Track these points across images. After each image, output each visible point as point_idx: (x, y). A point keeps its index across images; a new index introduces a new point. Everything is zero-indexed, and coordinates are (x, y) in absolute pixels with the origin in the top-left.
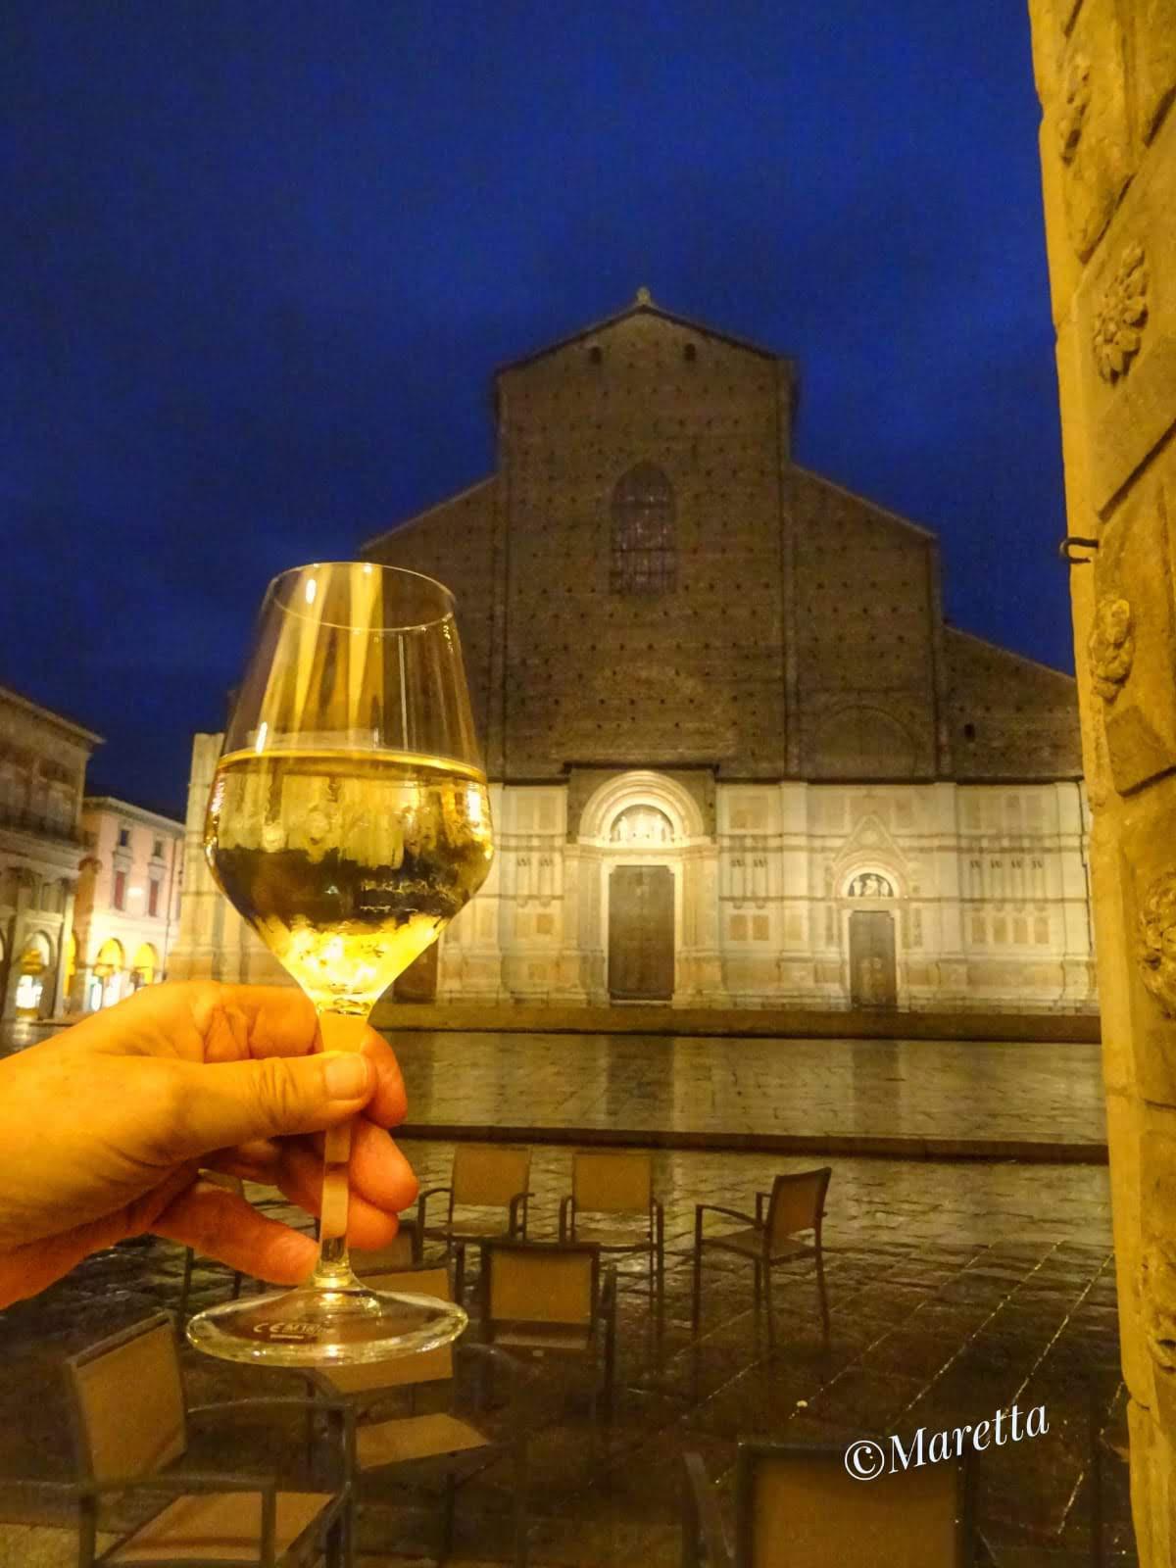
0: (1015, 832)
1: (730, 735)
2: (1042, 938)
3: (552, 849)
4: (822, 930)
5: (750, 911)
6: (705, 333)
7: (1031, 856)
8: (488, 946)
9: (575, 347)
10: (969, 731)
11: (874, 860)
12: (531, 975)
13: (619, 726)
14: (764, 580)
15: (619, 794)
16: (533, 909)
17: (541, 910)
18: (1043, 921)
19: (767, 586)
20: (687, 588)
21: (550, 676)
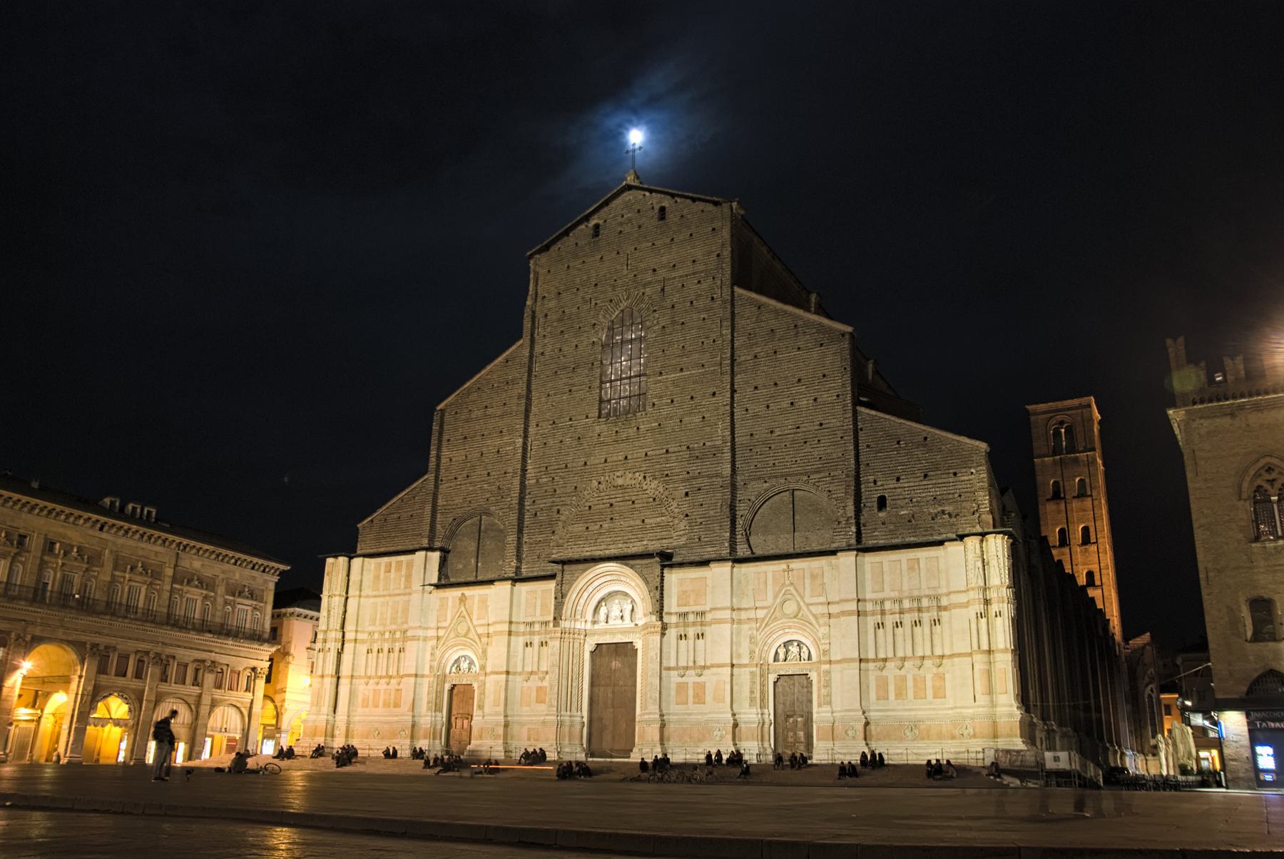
0: (916, 593)
1: (682, 526)
2: (939, 693)
3: (546, 633)
4: (746, 693)
5: (691, 678)
6: (673, 196)
7: (930, 614)
8: (497, 714)
9: (583, 227)
10: (882, 503)
11: (790, 627)
12: (529, 739)
13: (601, 526)
14: (711, 390)
15: (596, 584)
16: (534, 682)
17: (540, 684)
18: (941, 677)
19: (714, 394)
20: (654, 404)
21: (555, 491)
